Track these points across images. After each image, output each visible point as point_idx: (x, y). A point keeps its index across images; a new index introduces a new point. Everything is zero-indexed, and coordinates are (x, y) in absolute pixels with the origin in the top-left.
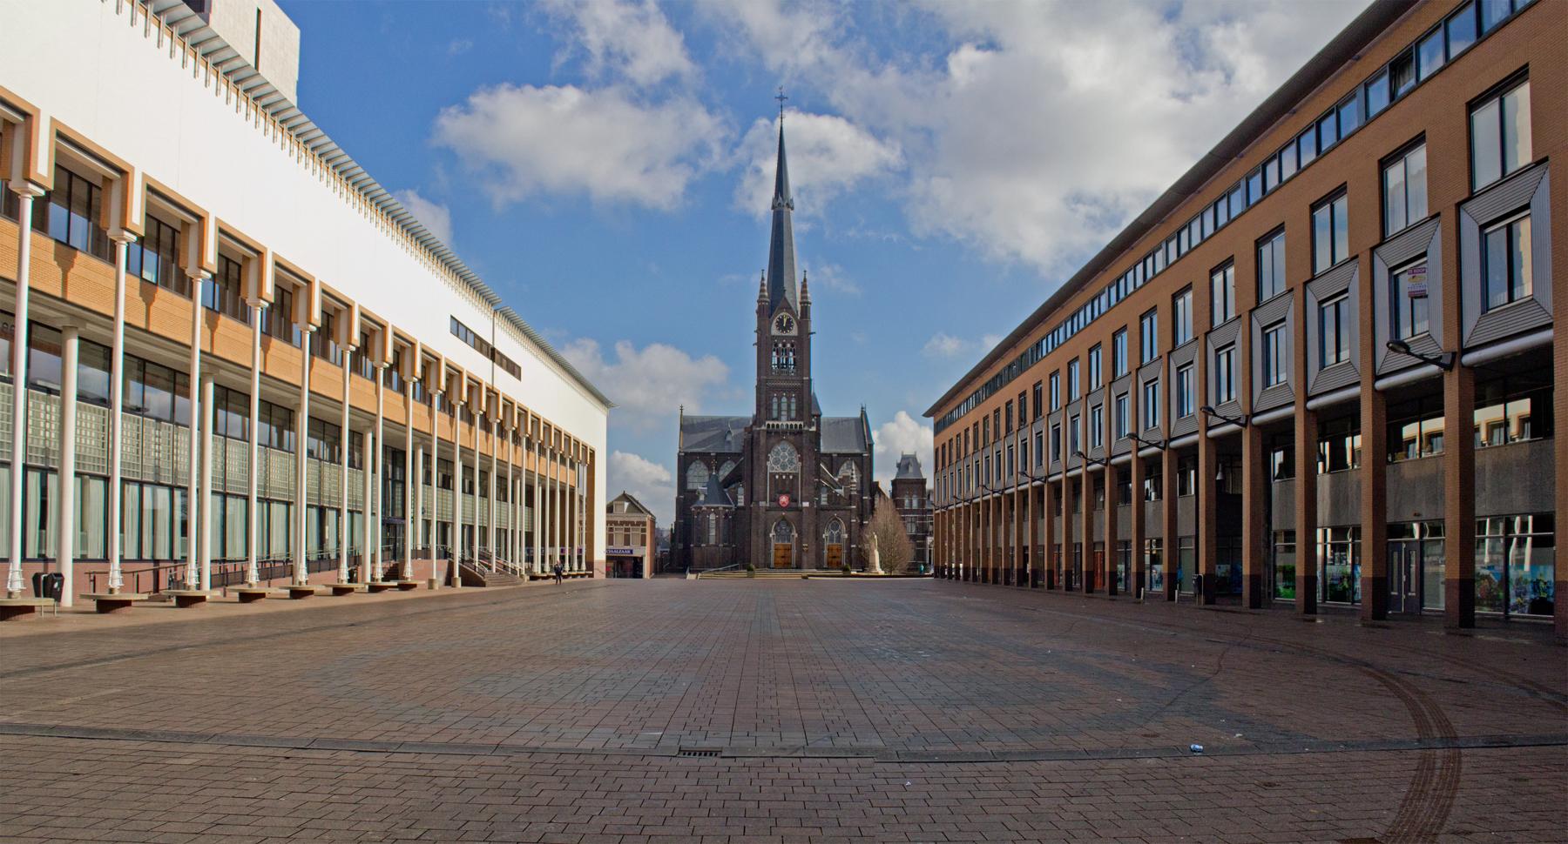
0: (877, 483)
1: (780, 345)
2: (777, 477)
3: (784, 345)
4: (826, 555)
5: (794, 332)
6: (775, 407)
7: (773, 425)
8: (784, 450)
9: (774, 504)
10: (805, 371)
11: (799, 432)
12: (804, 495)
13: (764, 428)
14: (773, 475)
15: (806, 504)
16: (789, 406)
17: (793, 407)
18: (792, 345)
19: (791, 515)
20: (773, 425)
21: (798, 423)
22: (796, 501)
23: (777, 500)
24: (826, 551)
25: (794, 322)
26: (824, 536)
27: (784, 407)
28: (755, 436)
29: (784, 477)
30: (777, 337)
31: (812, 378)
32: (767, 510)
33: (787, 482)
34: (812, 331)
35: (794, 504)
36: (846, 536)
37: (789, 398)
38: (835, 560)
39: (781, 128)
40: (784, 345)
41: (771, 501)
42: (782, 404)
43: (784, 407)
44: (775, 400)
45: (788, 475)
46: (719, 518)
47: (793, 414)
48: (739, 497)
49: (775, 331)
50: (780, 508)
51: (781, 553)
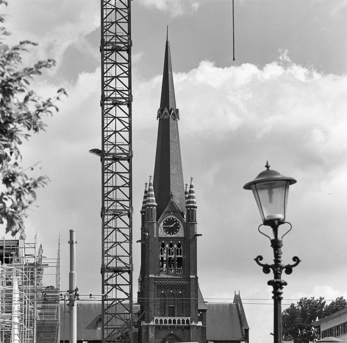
1: (167, 246)
5: (181, 233)
10: (192, 269)
13: (152, 323)
18: (179, 246)
21: (185, 319)
25: (181, 224)
28: (144, 331)
31: (198, 276)
34: (198, 233)
39: (167, 42)
49: (162, 233)
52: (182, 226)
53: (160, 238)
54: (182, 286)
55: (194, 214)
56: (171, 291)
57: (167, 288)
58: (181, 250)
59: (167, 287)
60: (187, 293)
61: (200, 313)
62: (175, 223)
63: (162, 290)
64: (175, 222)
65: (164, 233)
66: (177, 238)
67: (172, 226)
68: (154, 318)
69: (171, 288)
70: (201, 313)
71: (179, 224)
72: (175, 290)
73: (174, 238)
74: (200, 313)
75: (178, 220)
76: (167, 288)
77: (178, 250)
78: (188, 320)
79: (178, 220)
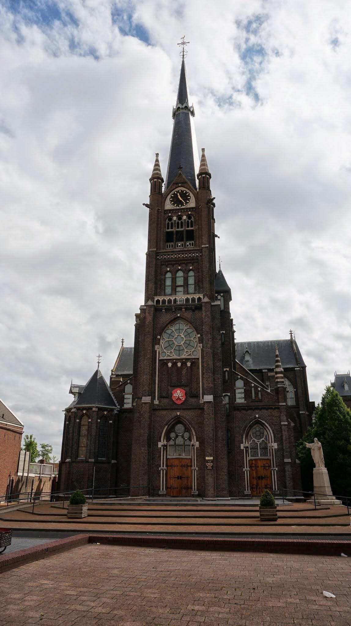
1: (175, 218)
2: (170, 365)
3: (180, 218)
4: (247, 476)
5: (192, 204)
6: (168, 282)
7: (164, 301)
9: (166, 401)
11: (197, 307)
12: (206, 385)
14: (164, 363)
15: (209, 398)
16: (186, 279)
17: (191, 281)
18: (189, 217)
19: (189, 415)
20: (164, 301)
21: (196, 296)
22: (197, 396)
23: (169, 396)
24: (247, 469)
25: (191, 195)
26: (242, 448)
27: (180, 282)
29: (179, 364)
30: (170, 211)
32: (155, 410)
33: (184, 372)
35: (193, 401)
36: (275, 445)
37: (186, 272)
38: (263, 482)
40: (180, 218)
41: (161, 397)
43: (180, 282)
44: (169, 275)
45: (184, 362)
46: (91, 422)
47: (191, 289)
48: (126, 396)
50: (174, 406)
51: (176, 472)
52: (193, 195)
53: (167, 210)
54: (193, 259)
56: (180, 268)
57: (174, 264)
58: (192, 221)
59: (173, 263)
60: (199, 267)
61: (221, 295)
63: (167, 267)
65: (172, 206)
66: (187, 208)
69: (178, 264)
70: (222, 294)
71: (189, 196)
72: (184, 265)
73: (184, 209)
75: (188, 191)
76: (174, 264)
77: (188, 221)
78: (199, 299)
79: (188, 191)
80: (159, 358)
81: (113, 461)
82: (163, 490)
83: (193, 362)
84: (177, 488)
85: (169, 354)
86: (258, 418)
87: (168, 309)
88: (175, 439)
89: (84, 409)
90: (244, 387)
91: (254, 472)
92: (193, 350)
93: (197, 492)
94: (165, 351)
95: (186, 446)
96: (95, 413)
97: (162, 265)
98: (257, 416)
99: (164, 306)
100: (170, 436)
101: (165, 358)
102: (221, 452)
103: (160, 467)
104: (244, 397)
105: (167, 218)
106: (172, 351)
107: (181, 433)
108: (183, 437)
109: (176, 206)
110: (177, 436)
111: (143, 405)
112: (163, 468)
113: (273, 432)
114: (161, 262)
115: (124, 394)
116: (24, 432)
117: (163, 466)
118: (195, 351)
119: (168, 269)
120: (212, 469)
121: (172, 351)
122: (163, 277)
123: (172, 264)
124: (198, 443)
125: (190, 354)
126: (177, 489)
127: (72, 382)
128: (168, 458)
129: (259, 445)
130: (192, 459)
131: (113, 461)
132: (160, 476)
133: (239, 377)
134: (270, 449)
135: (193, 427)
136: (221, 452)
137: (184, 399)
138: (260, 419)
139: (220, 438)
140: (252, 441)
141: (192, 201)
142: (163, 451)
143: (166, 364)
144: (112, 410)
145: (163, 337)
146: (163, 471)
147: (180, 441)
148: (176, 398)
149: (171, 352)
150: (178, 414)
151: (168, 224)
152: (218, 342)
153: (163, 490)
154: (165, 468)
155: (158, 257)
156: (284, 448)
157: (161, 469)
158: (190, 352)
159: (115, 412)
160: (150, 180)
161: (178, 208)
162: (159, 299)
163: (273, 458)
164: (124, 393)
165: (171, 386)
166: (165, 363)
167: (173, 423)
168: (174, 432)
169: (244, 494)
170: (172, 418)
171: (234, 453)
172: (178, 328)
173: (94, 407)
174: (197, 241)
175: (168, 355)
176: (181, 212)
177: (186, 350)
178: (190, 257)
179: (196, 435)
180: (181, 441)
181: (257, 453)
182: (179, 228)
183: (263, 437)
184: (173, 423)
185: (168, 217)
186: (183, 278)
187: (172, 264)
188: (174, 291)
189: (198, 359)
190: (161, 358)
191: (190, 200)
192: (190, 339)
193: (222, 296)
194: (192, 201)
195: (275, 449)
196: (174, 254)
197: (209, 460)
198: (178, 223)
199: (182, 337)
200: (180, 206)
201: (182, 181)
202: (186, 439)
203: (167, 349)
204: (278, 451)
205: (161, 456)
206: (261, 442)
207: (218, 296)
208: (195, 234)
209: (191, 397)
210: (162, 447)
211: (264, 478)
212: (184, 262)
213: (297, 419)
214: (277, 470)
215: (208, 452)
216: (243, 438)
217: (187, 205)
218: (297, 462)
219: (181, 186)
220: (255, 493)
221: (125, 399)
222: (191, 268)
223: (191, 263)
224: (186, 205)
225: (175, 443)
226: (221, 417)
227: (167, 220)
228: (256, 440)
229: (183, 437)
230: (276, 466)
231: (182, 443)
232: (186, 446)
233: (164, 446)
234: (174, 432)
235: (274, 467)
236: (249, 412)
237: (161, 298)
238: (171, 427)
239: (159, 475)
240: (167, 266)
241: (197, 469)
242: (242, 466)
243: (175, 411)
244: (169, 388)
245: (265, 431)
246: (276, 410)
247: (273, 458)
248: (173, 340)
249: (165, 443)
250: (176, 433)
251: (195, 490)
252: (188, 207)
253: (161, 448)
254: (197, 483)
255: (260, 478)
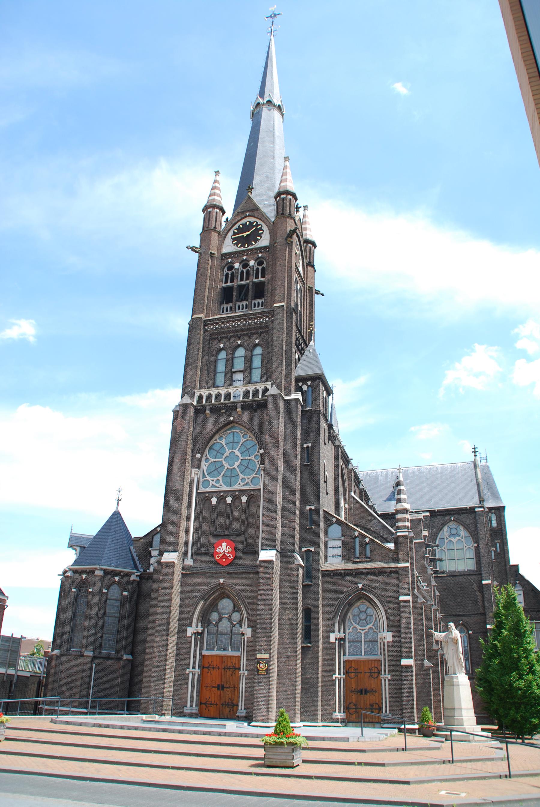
0: (517, 566)
2: (214, 501)
3: (245, 265)
5: (264, 241)
6: (221, 367)
8: (233, 444)
9: (204, 559)
16: (249, 361)
17: (257, 362)
18: (260, 263)
23: (209, 552)
25: (265, 228)
27: (239, 364)
29: (229, 500)
30: (230, 254)
33: (237, 512)
35: (247, 559)
36: (389, 637)
40: (245, 265)
42: (236, 361)
43: (239, 364)
44: (223, 355)
45: (236, 495)
47: (256, 375)
51: (214, 677)
53: (226, 254)
54: (261, 328)
55: (286, 204)
56: (239, 342)
57: (231, 337)
59: (229, 335)
60: (270, 340)
61: (307, 385)
62: (254, 228)
64: (254, 226)
67: (249, 233)
68: (194, 393)
70: (309, 383)
71: (261, 229)
72: (246, 338)
73: (251, 250)
74: (307, 385)
75: (260, 222)
76: (231, 337)
79: (260, 222)
80: (198, 488)
81: (125, 657)
82: (191, 705)
83: (251, 496)
84: (216, 705)
85: (214, 483)
86: (362, 589)
87: (215, 410)
88: (217, 623)
89: (83, 571)
90: (343, 535)
91: (353, 681)
92: (253, 475)
93: (245, 712)
94: (208, 478)
95: (235, 634)
96: (98, 579)
97: (212, 339)
98: (360, 586)
99: (209, 405)
100: (209, 620)
101: (208, 489)
102: (287, 646)
103: (189, 668)
104: (340, 553)
105: (226, 265)
106: (220, 478)
107: (227, 614)
108: (230, 619)
109: (240, 247)
110: (220, 619)
111: (164, 566)
112: (194, 670)
113: (386, 613)
114: (211, 335)
115: (150, 549)
116: (7, 606)
117: (194, 667)
118: (256, 477)
119: (222, 346)
120: (267, 674)
121: (220, 478)
122: (213, 359)
123: (226, 337)
124: (250, 630)
125: (248, 482)
126: (215, 706)
127: (72, 530)
128: (203, 654)
129: (363, 635)
130: (241, 657)
131: (125, 657)
132: (188, 683)
133: (334, 520)
134: (381, 643)
135: (243, 603)
136: (287, 646)
137: (232, 557)
138: (365, 591)
139: (288, 623)
140: (353, 628)
141: (264, 237)
142: (196, 643)
143: (209, 499)
144: (128, 575)
145: (206, 456)
146: (193, 675)
147: (225, 625)
148: (220, 555)
149: (218, 480)
150: (222, 582)
151: (227, 275)
152: (292, 461)
153: (191, 705)
154: (197, 670)
155: (206, 328)
156: (403, 640)
157: (189, 672)
158: (248, 479)
159: (133, 577)
160: (204, 210)
161: (243, 249)
162: (203, 394)
163: (385, 658)
164: (152, 547)
165: (214, 536)
166: (206, 498)
167: (214, 596)
168: (217, 611)
169: (331, 718)
170: (212, 589)
171: (316, 649)
172: (231, 441)
173: (96, 569)
174: (269, 298)
175: (212, 484)
176: (247, 255)
177: (241, 476)
178: (255, 323)
179: (247, 617)
180: (226, 627)
181: (359, 649)
182: (243, 280)
183: (371, 623)
184: (214, 596)
185: (227, 264)
186: (243, 359)
187: (226, 337)
188: (229, 380)
189: (260, 490)
190: (201, 490)
191: (263, 236)
192: (248, 458)
193: (309, 386)
194: (264, 237)
195: (388, 643)
196: (232, 321)
197: (263, 659)
198: (242, 272)
199: (237, 456)
200: (246, 245)
201: (252, 208)
202: (235, 623)
203: (212, 474)
204: (392, 645)
205: (190, 651)
206: (367, 630)
207: (303, 385)
208: (266, 288)
209: (244, 553)
210: (193, 636)
211: (369, 692)
212: (247, 333)
213: (478, 593)
214: (389, 678)
215: (261, 646)
216: (334, 623)
217: (257, 244)
218: (425, 665)
219: (249, 216)
220: (354, 716)
221: (152, 557)
222: (257, 341)
223: (257, 333)
224: (255, 243)
225: (217, 630)
226: (291, 588)
227: (226, 269)
228: (359, 627)
229: (230, 619)
230: (389, 671)
231: (229, 629)
232: (235, 634)
233: (196, 634)
234: (217, 611)
235: (385, 674)
236: (347, 579)
237: (205, 393)
238: (210, 602)
239: (187, 681)
240: (220, 341)
241: (246, 674)
242: (330, 671)
243: (217, 576)
244: (211, 538)
245: (375, 612)
246: (394, 576)
247: (385, 658)
248: (221, 460)
249: (200, 629)
250: (219, 614)
251: (241, 709)
252: (258, 246)
253: (192, 636)
254: (245, 697)
255: (364, 692)
